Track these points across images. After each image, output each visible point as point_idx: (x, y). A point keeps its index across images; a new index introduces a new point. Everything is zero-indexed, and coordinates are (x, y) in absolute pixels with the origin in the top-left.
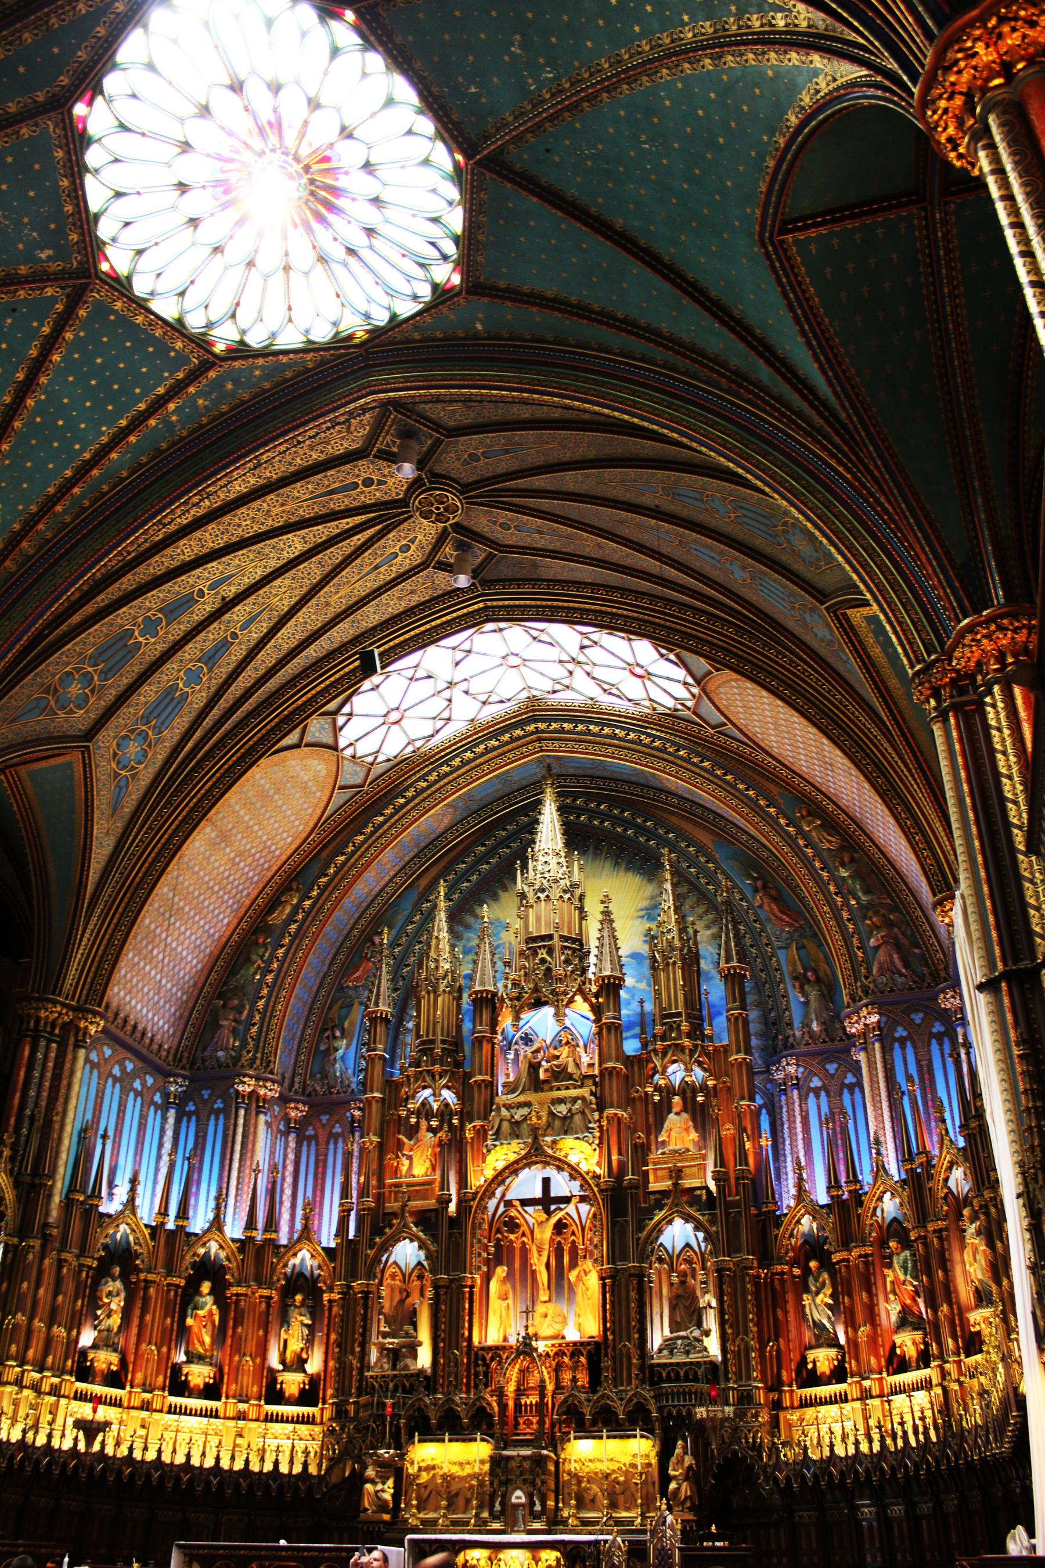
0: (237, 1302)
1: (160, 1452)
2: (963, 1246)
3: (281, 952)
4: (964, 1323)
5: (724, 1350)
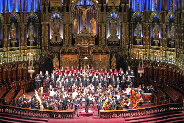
0: (20, 27)
2: (170, 30)
4: (168, 42)
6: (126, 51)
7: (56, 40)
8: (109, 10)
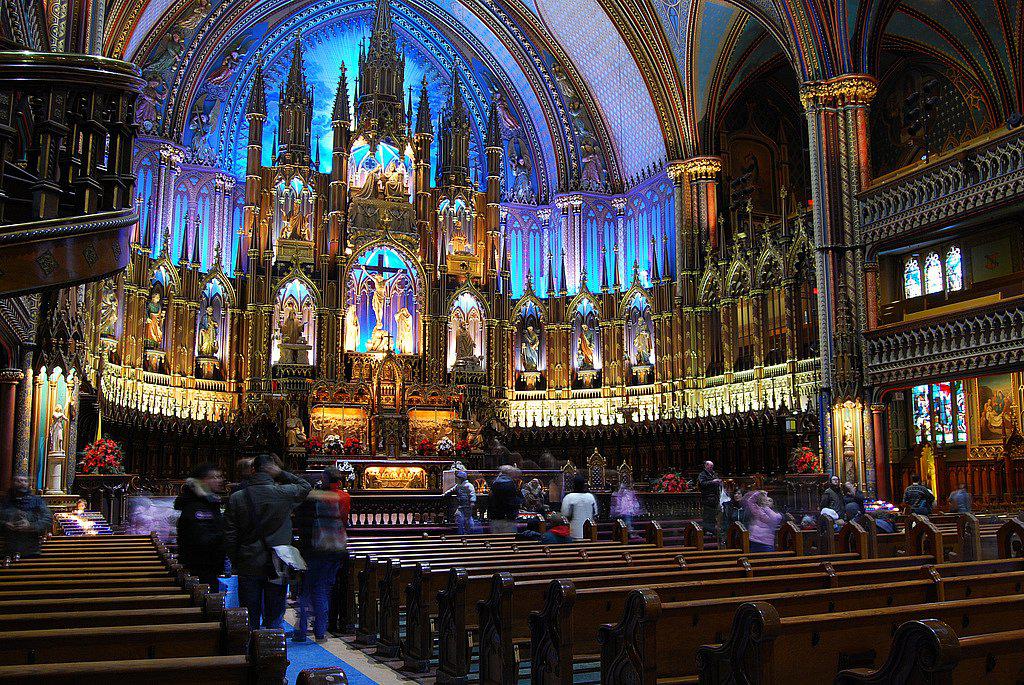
1: (161, 409)
3: (191, 53)
5: (489, 367)
6: (505, 404)
7: (295, 360)
8: (452, 285)
